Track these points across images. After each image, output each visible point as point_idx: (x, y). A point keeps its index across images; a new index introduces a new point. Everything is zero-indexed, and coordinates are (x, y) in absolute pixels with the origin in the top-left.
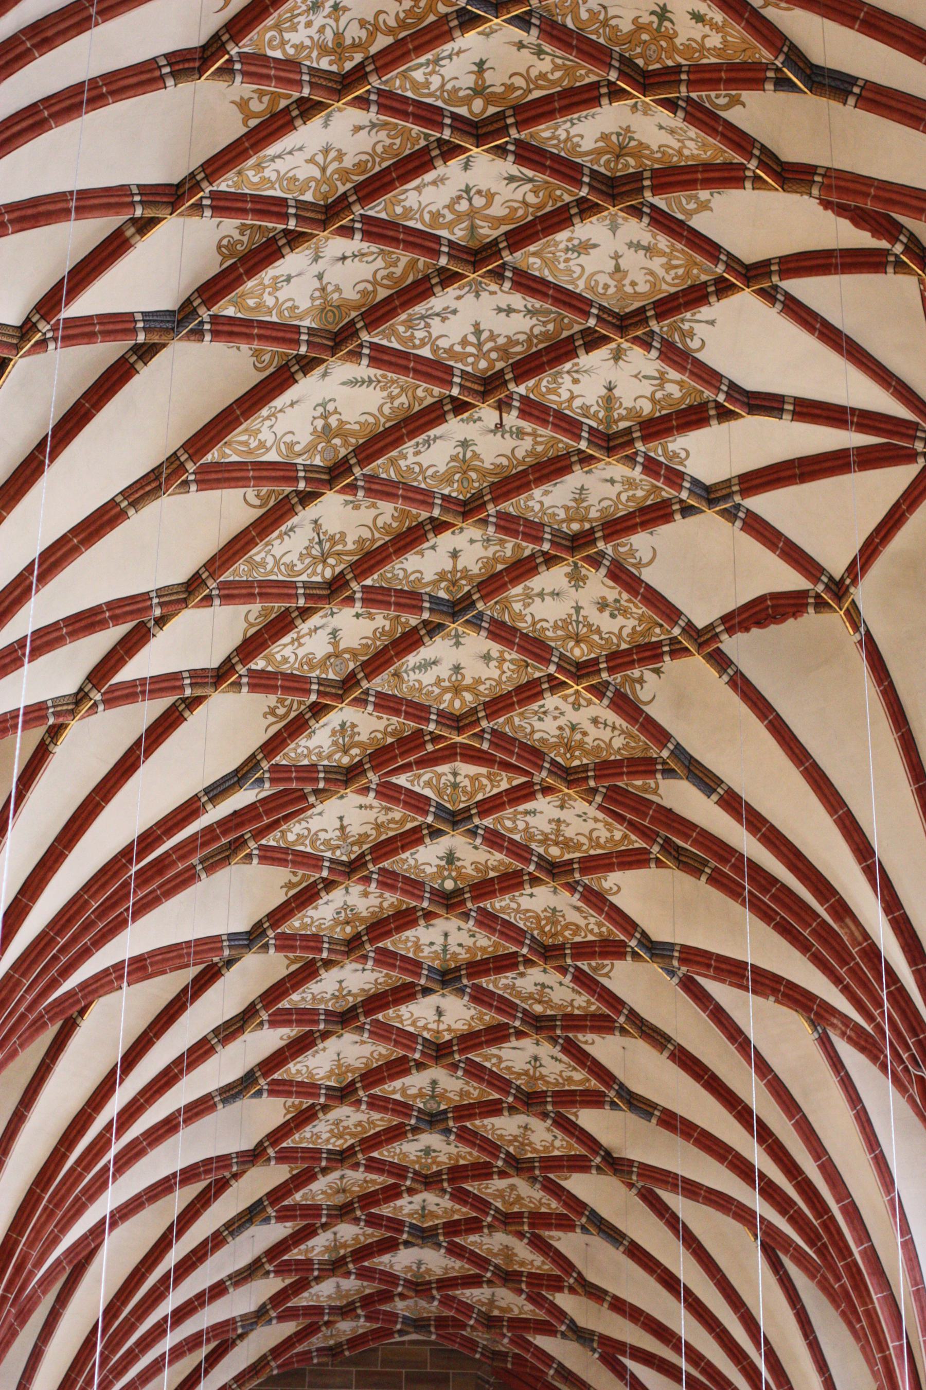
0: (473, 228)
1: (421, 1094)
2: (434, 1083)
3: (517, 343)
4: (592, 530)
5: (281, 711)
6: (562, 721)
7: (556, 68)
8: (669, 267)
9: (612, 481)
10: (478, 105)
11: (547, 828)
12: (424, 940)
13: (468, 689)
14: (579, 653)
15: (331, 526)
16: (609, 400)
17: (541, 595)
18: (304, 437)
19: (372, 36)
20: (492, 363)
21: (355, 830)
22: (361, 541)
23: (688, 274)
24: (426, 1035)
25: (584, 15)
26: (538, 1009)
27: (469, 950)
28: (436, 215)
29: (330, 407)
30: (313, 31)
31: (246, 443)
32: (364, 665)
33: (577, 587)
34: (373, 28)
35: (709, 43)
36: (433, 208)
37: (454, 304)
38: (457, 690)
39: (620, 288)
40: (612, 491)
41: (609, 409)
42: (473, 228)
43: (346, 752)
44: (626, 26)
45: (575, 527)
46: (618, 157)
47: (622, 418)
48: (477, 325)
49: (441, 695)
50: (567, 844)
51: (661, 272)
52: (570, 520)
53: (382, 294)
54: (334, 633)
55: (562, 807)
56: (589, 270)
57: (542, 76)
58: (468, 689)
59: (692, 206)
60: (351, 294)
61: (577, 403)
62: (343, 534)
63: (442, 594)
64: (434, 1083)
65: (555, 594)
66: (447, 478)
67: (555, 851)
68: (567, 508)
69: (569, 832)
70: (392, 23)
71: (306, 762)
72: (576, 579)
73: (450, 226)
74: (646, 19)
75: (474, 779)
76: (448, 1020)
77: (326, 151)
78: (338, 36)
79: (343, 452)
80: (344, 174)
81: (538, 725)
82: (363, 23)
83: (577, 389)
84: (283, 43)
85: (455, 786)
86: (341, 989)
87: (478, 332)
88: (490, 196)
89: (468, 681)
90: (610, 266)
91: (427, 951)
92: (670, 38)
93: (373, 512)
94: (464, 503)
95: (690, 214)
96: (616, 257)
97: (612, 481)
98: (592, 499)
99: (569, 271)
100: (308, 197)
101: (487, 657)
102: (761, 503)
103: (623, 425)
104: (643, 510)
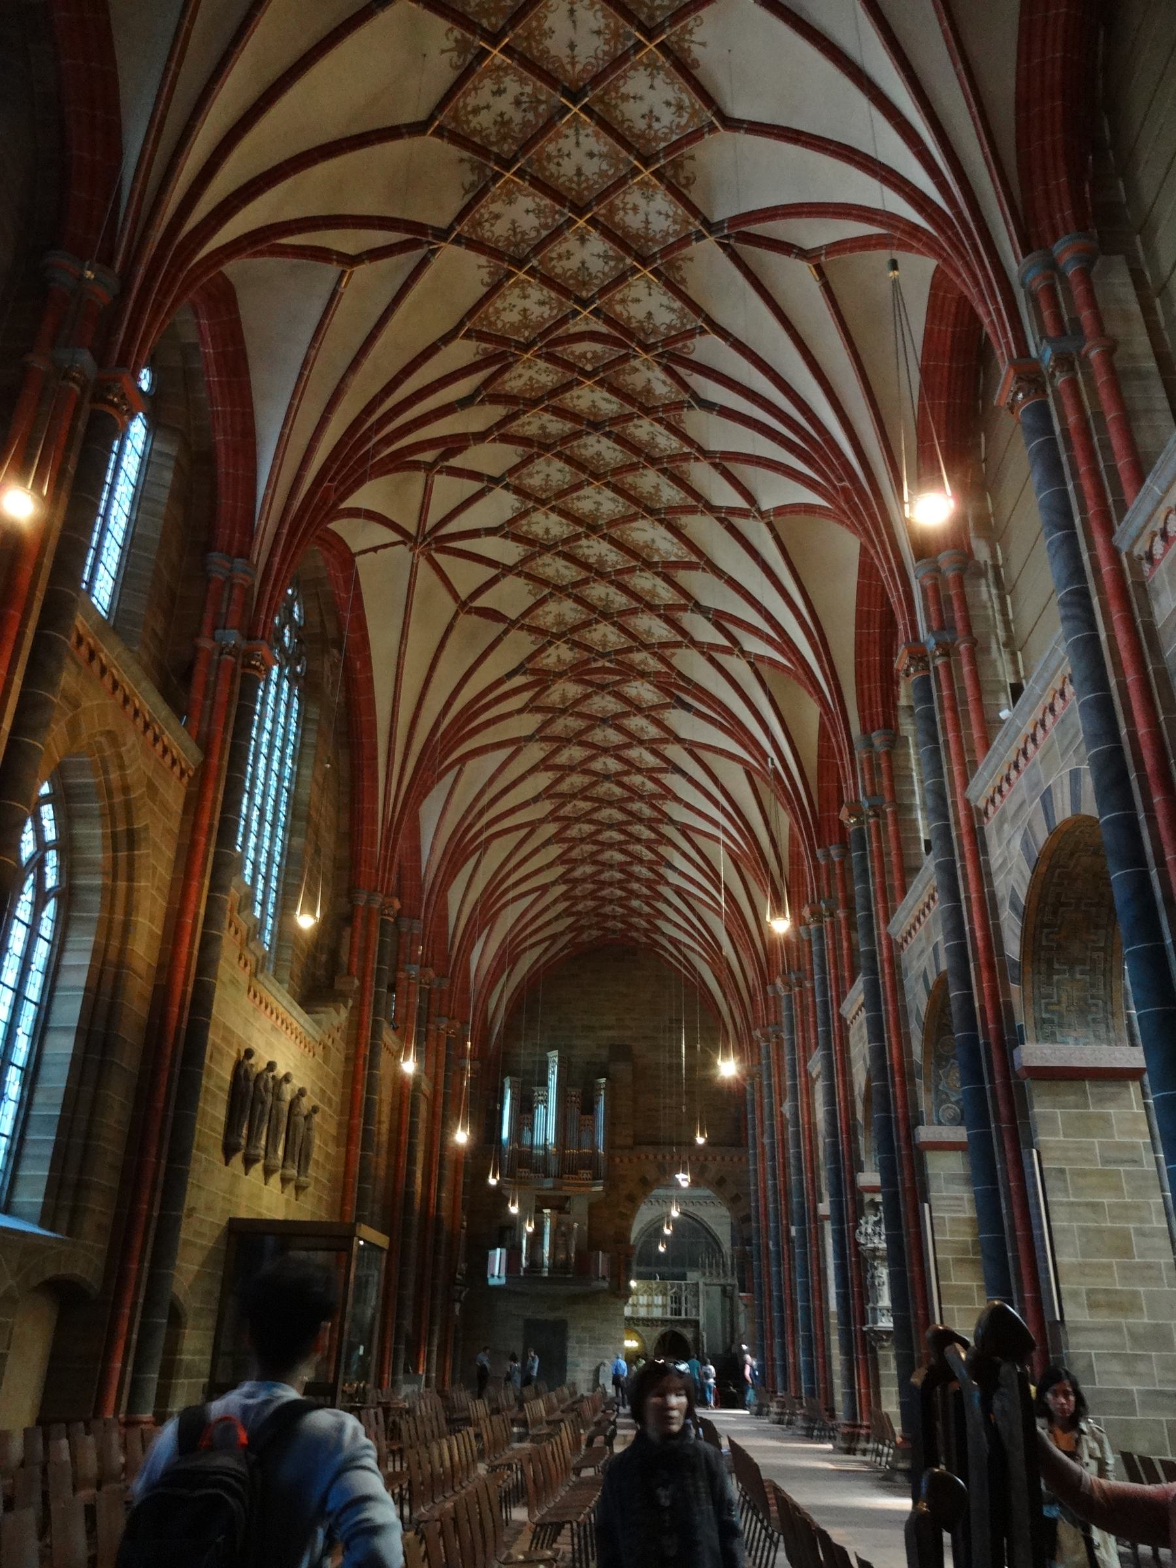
6: (536, 368)
9: (538, 472)
11: (530, 291)
40: (537, 468)
55: (525, 310)
101: (579, 397)
102: (493, 572)
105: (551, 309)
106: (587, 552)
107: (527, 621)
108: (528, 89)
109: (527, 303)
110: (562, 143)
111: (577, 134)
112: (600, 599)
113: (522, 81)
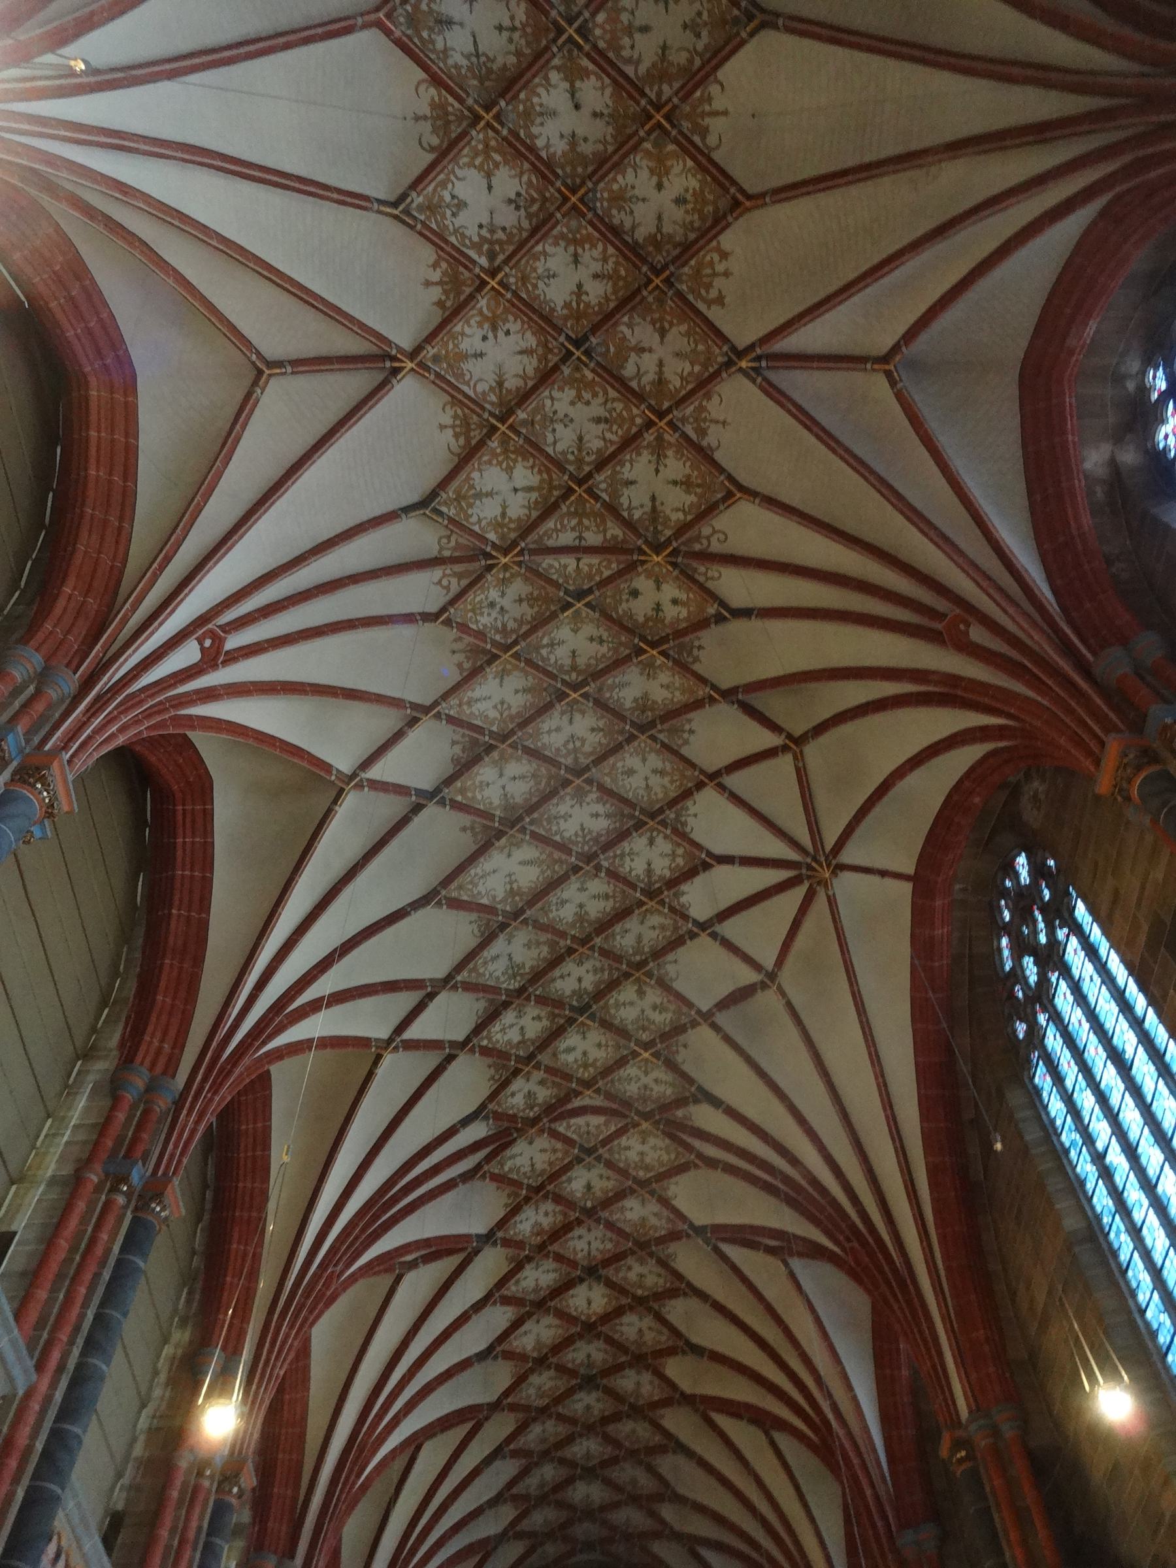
0: (576, 759)
1: (582, 1364)
2: (589, 1356)
3: (602, 835)
4: (646, 959)
5: (497, 1077)
7: (609, 650)
8: (672, 782)
10: (574, 675)
12: (578, 1248)
13: (591, 1065)
14: (645, 1037)
15: (518, 959)
16: (649, 871)
17: (624, 1004)
18: (500, 894)
19: (520, 626)
20: (590, 848)
21: (539, 1167)
22: (532, 968)
23: (681, 784)
24: (583, 1318)
25: (620, 612)
26: (639, 1292)
27: (601, 1252)
28: (558, 750)
29: (513, 878)
30: (491, 619)
31: (471, 890)
32: (538, 1048)
33: (641, 999)
34: (521, 622)
35: (681, 617)
36: (557, 745)
37: (570, 811)
38: (586, 1066)
39: (649, 795)
41: (649, 877)
42: (576, 759)
43: (532, 1108)
44: (641, 619)
45: (638, 958)
46: (643, 712)
47: (656, 882)
48: (582, 825)
49: (578, 1068)
50: (647, 1168)
51: (668, 785)
52: (634, 954)
53: (535, 800)
54: (522, 1028)
56: (634, 786)
57: (604, 656)
58: (591, 1065)
59: (680, 742)
60: (519, 800)
61: (633, 873)
62: (524, 964)
63: (575, 1003)
64: (589, 1356)
65: (632, 1004)
66: (573, 925)
67: (641, 1173)
68: (633, 948)
69: (648, 1160)
70: (529, 618)
71: (511, 1112)
72: (641, 993)
73: (565, 756)
74: (650, 613)
75: (598, 1127)
76: (594, 1306)
77: (502, 703)
78: (504, 625)
79: (520, 905)
80: (512, 718)
81: (628, 1088)
82: (515, 620)
83: (633, 865)
84: (477, 622)
85: (588, 1133)
86: (537, 1285)
87: (583, 829)
88: (583, 741)
89: (591, 1061)
90: (643, 785)
91: (580, 1255)
92: (663, 621)
93: (538, 951)
94: (582, 940)
95: (680, 747)
96: (646, 779)
97: (654, 928)
98: (645, 941)
99: (624, 786)
100: (494, 729)
103: (657, 885)
104: (670, 943)
105: (619, 1144)
106: (600, 808)
107: (702, 692)
108: (621, 1275)
109: (639, 1147)
110: (601, 1247)
111: (589, 1254)
112: (583, 713)
113: (625, 1279)
